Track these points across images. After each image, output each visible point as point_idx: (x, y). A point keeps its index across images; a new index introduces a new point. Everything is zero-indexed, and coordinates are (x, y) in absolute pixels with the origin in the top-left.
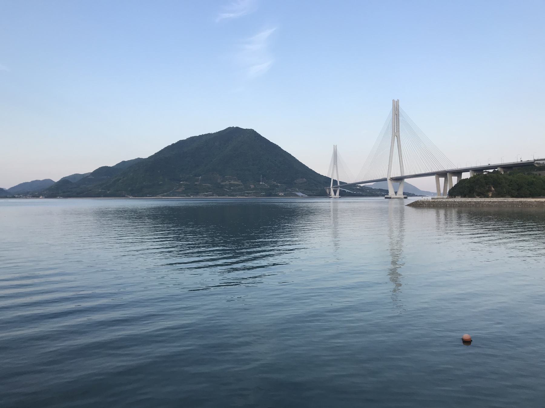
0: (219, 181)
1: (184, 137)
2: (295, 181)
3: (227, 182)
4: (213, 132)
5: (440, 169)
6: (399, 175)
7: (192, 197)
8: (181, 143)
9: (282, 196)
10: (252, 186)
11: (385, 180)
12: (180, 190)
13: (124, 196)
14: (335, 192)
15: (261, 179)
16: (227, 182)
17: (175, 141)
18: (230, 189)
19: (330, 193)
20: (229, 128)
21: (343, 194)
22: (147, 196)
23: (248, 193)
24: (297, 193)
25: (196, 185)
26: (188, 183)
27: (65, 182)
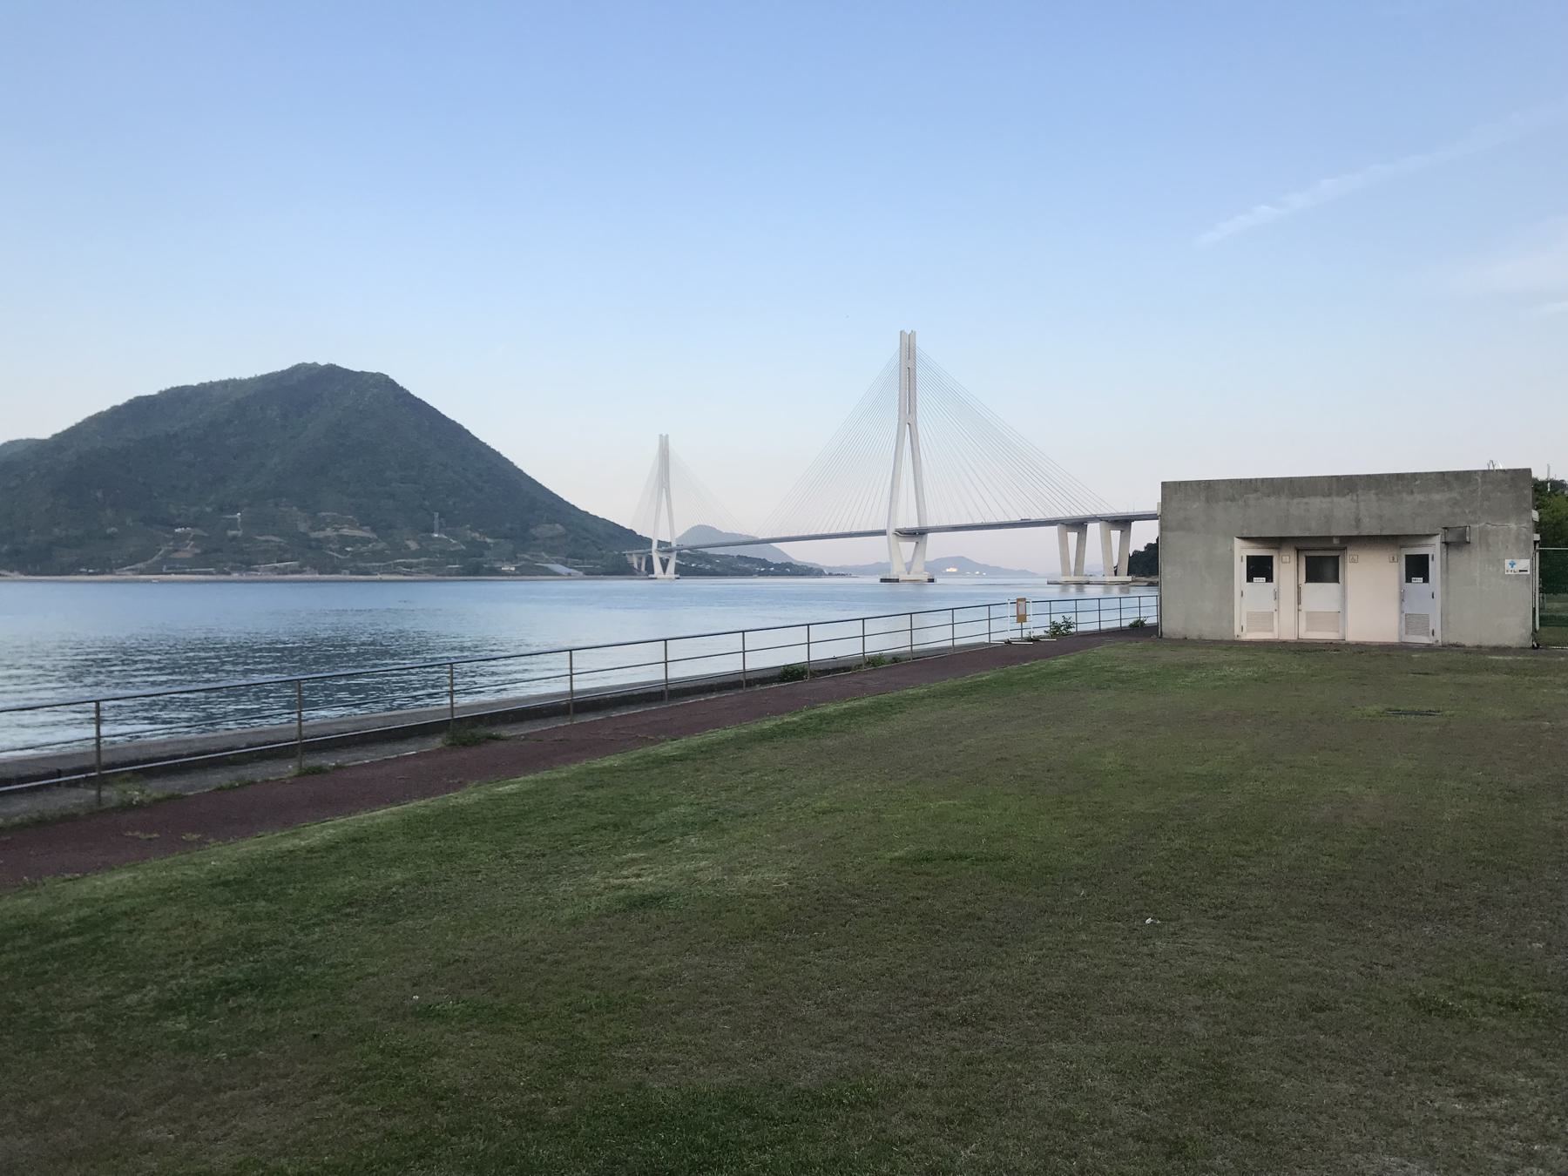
0: (302, 527)
1: (151, 387)
2: (533, 531)
3: (329, 532)
4: (246, 377)
6: (914, 525)
7: (235, 576)
8: (140, 409)
10: (413, 545)
11: (883, 533)
12: (187, 552)
16: (329, 532)
17: (121, 399)
18: (341, 551)
21: (682, 571)
22: (81, 573)
23: (409, 566)
25: (234, 538)
26: (199, 532)
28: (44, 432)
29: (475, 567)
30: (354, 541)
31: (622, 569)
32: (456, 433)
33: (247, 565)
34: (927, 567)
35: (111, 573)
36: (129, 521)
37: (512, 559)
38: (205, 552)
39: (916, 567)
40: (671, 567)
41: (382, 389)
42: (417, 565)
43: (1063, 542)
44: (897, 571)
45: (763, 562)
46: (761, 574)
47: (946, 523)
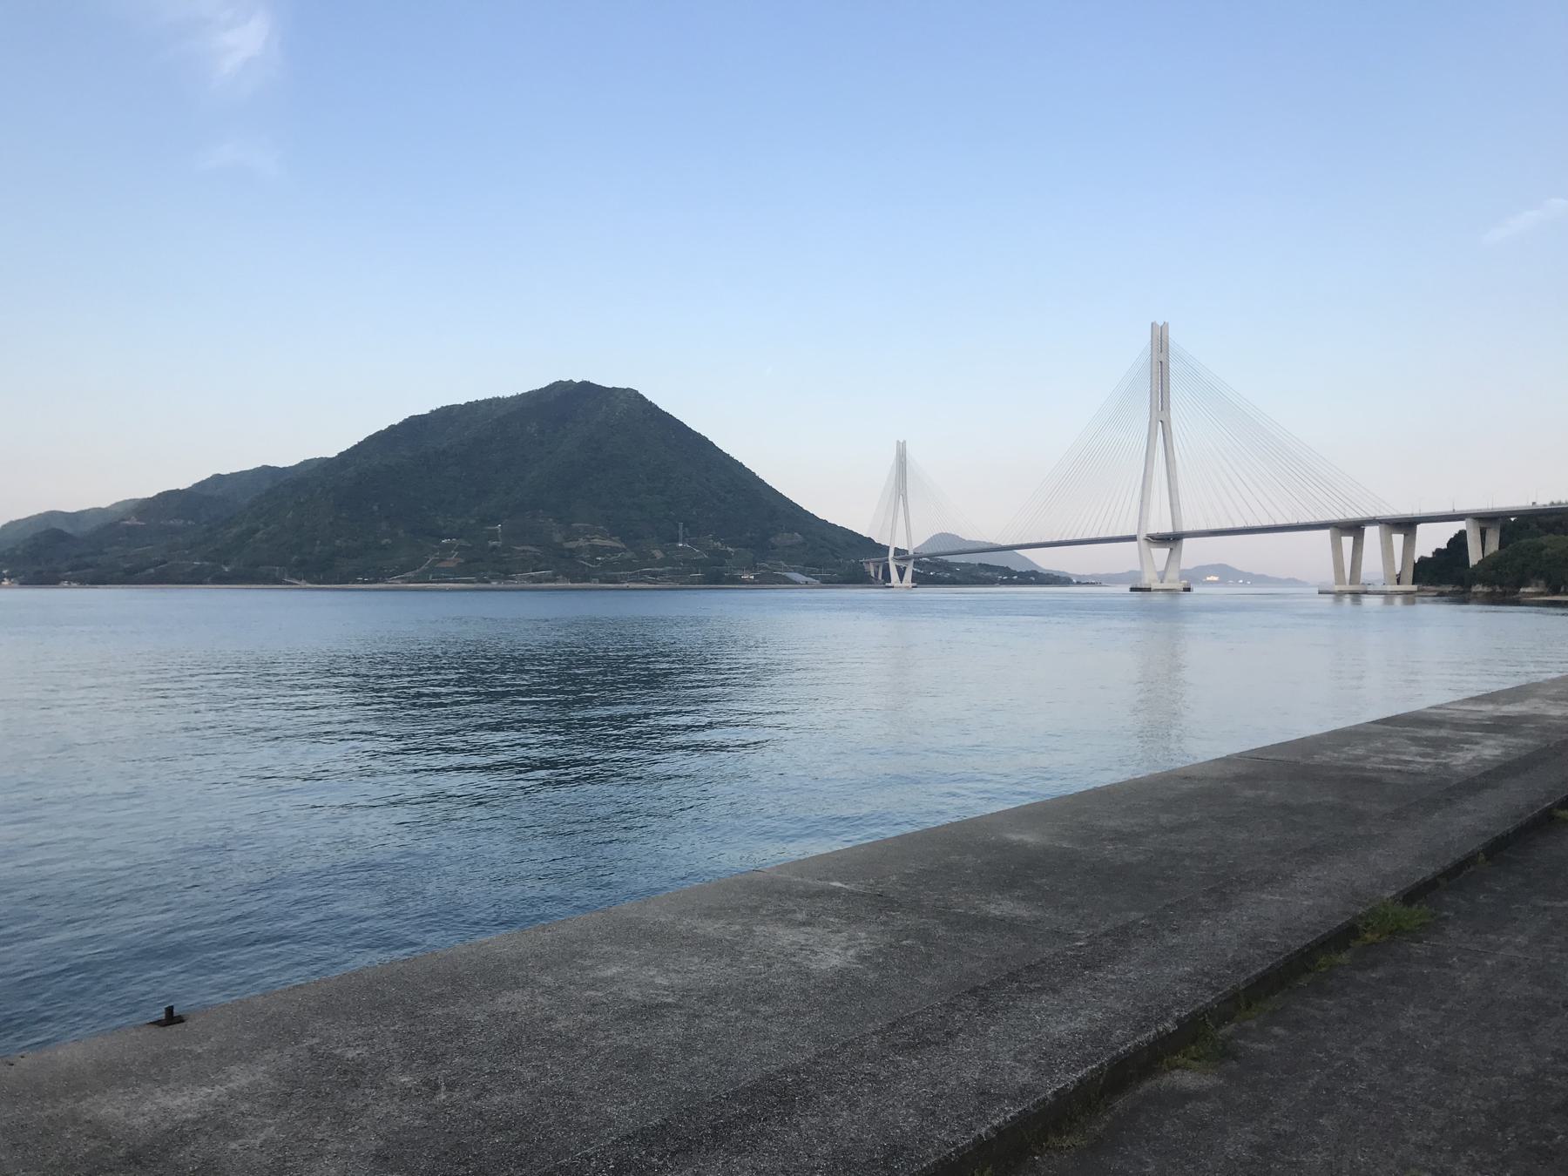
0: (557, 538)
2: (772, 540)
3: (582, 542)
4: (508, 395)
5: (1352, 514)
6: (1167, 529)
7: (494, 584)
8: (414, 426)
10: (659, 554)
12: (452, 561)
13: (277, 581)
16: (582, 542)
17: (396, 420)
21: (920, 580)
22: (357, 582)
23: (654, 575)
24: (789, 575)
25: (494, 548)
26: (463, 542)
28: (332, 453)
29: (716, 576)
30: (603, 550)
31: (859, 578)
32: (701, 444)
33: (506, 575)
34: (1184, 574)
35: (383, 582)
36: (401, 532)
37: (751, 568)
38: (468, 562)
39: (1172, 574)
40: (908, 575)
42: (661, 574)
43: (1337, 547)
44: (1149, 579)
45: (1006, 571)
46: (1003, 583)
47: (1203, 527)
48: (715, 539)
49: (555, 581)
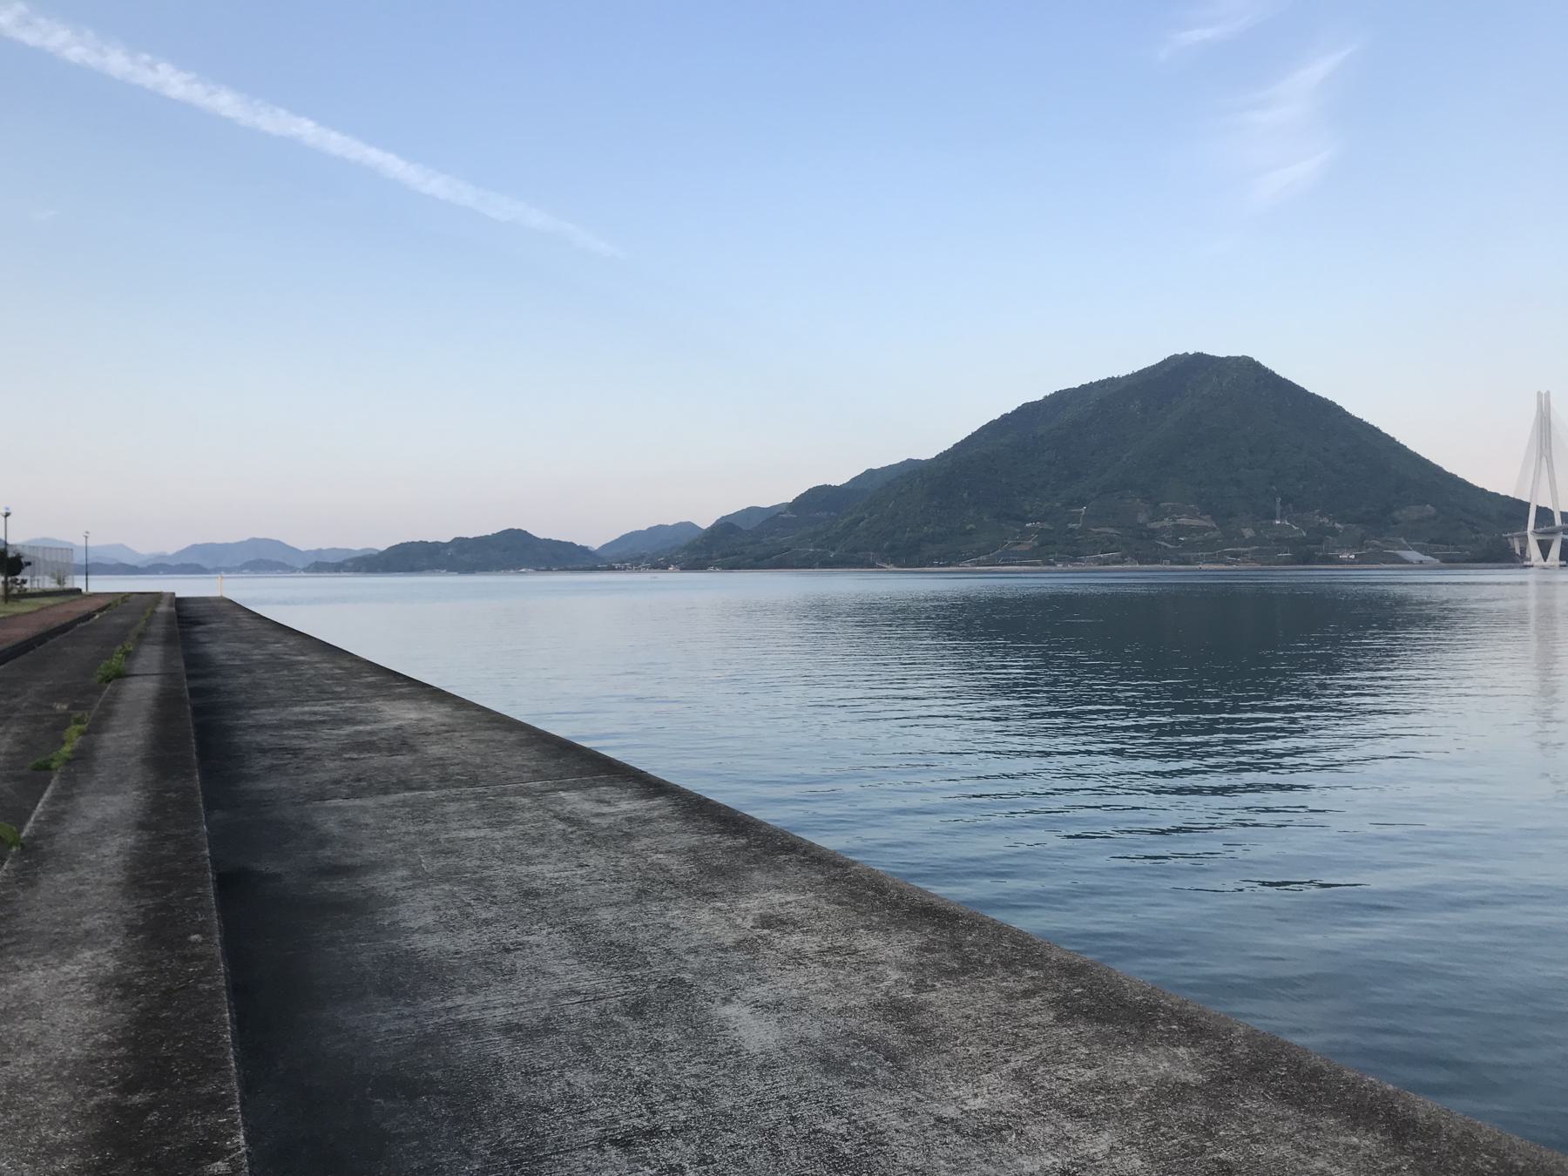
0: (1142, 518)
2: (1396, 514)
3: (1167, 522)
4: (1122, 374)
7: (1060, 566)
8: (1028, 412)
9: (1352, 562)
13: (872, 566)
14: (1545, 548)
15: (1278, 508)
16: (1167, 522)
18: (1176, 541)
19: (1523, 550)
20: (1174, 358)
23: (1236, 555)
25: (1072, 530)
27: (726, 527)
30: (1188, 530)
38: (1041, 545)
40: (1555, 551)
41: (1248, 372)
48: (1321, 515)
49: (1123, 562)
